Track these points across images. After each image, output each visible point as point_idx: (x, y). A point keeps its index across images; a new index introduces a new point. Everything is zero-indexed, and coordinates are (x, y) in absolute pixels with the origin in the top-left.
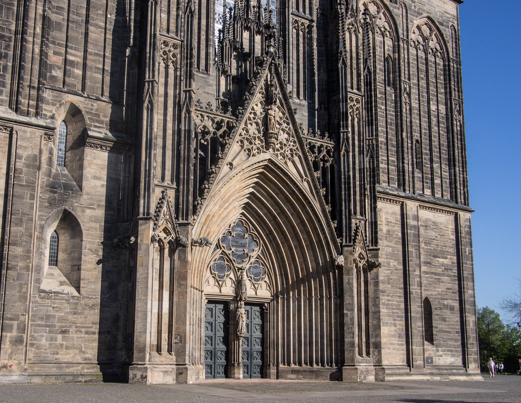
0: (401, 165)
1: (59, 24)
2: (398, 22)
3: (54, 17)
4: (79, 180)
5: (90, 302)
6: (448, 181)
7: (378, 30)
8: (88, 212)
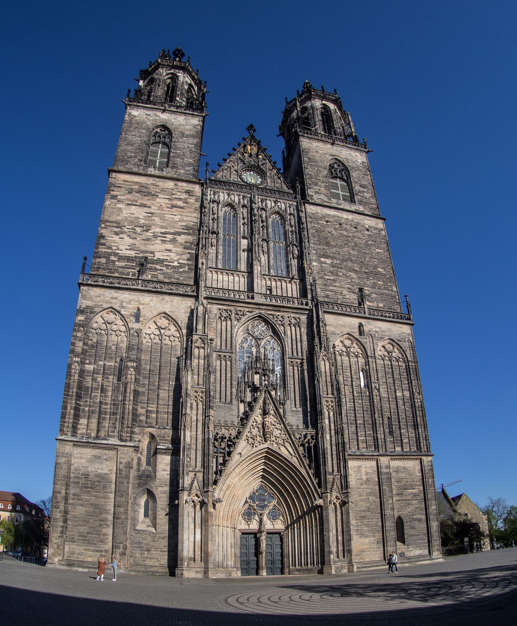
0: (376, 436)
1: (143, 393)
2: (366, 347)
3: (141, 389)
4: (155, 472)
5: (162, 536)
6: (414, 439)
7: (353, 355)
8: (160, 489)
